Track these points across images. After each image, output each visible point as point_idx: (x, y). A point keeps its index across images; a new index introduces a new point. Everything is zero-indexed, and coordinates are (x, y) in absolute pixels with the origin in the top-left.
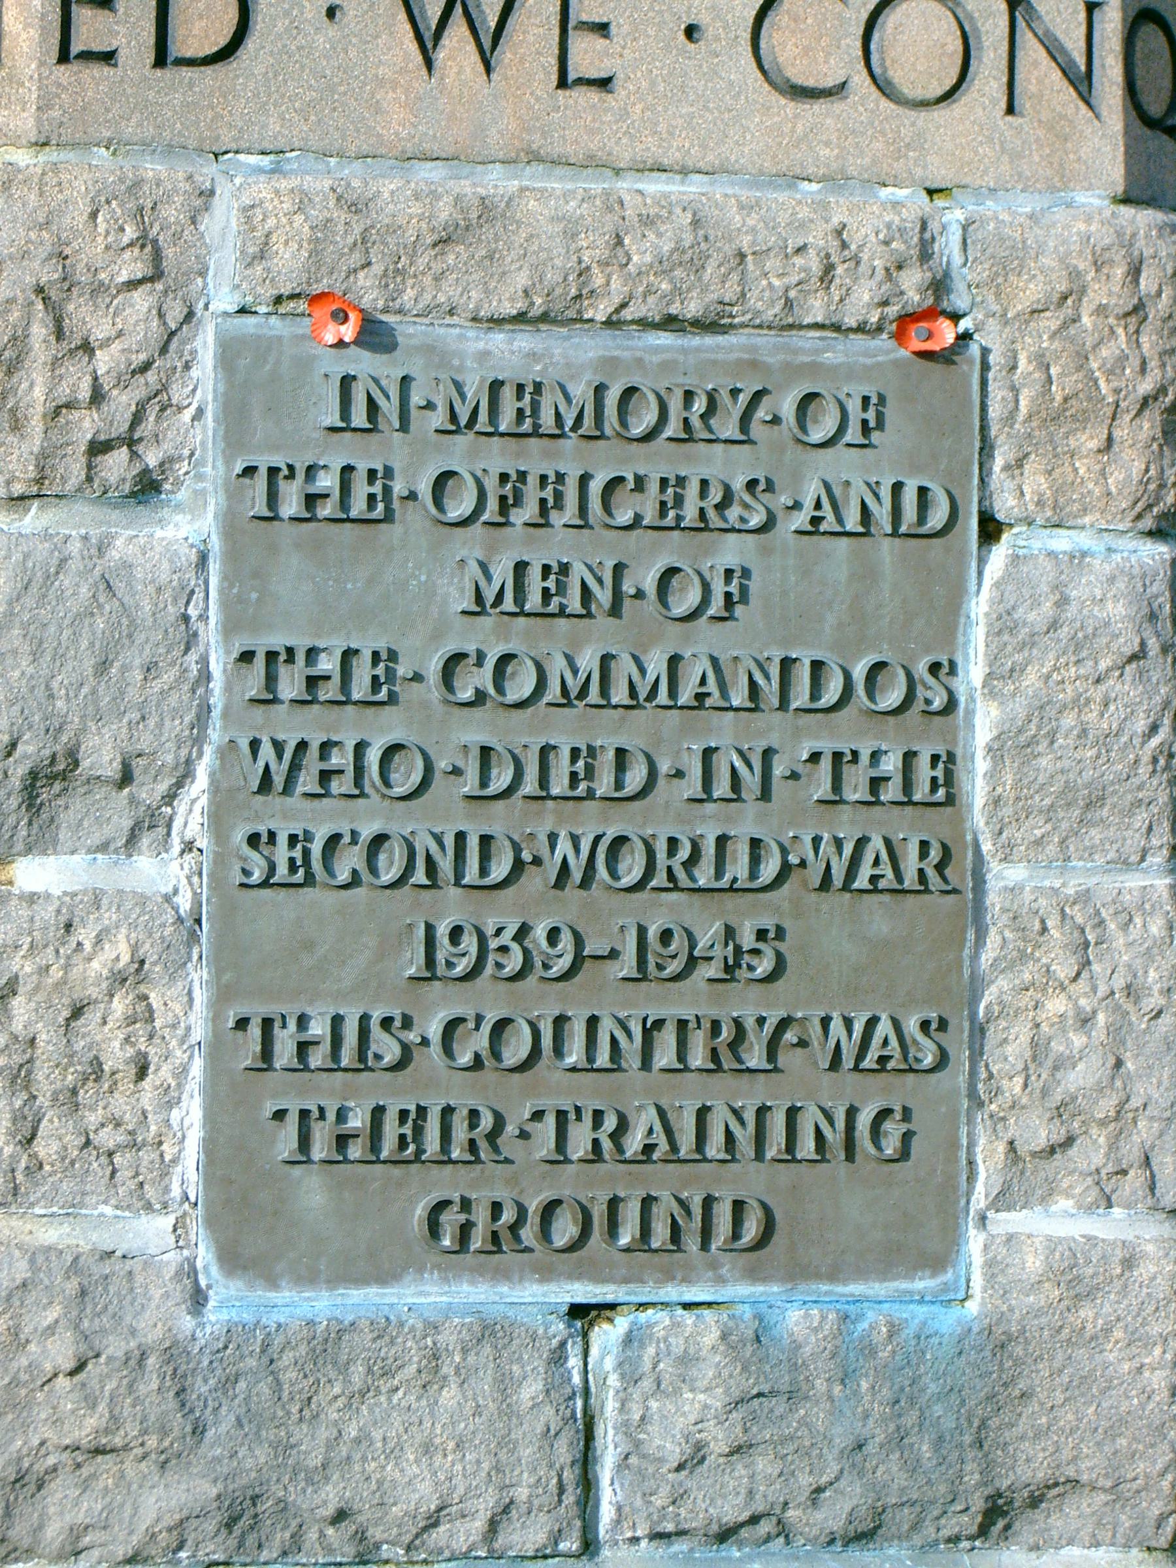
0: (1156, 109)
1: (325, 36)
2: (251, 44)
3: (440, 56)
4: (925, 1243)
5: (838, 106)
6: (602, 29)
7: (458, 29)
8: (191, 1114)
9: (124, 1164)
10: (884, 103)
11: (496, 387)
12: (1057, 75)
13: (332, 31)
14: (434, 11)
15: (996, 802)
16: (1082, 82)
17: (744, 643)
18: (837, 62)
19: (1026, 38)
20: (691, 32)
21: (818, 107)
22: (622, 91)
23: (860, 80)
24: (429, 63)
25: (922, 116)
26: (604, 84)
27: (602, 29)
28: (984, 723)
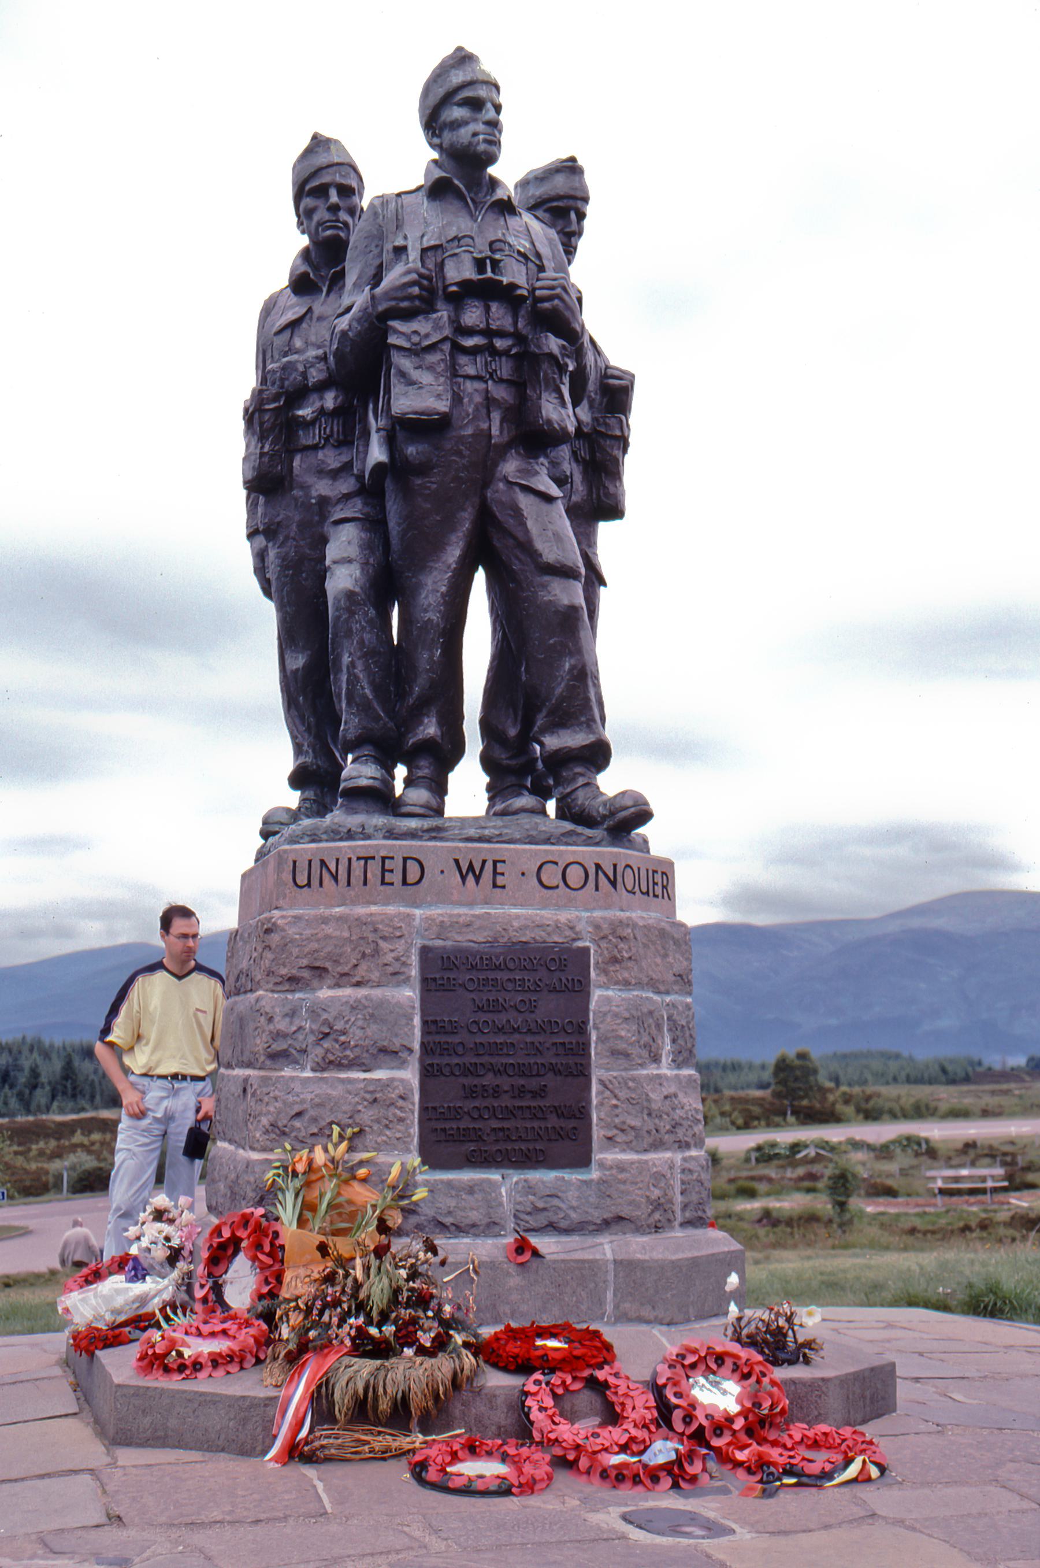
0: (629, 888)
1: (440, 877)
2: (424, 880)
3: (467, 882)
4: (583, 1161)
5: (556, 891)
6: (503, 874)
7: (470, 875)
8: (415, 1130)
9: (400, 1144)
10: (568, 890)
11: (481, 958)
12: (606, 881)
13: (442, 876)
14: (464, 872)
15: (596, 1054)
16: (613, 883)
17: (540, 1016)
18: (557, 880)
19: (600, 872)
20: (523, 874)
21: (550, 892)
22: (507, 888)
23: (562, 884)
24: (464, 883)
25: (575, 892)
26: (503, 887)
27: (503, 874)
28: (594, 1037)
